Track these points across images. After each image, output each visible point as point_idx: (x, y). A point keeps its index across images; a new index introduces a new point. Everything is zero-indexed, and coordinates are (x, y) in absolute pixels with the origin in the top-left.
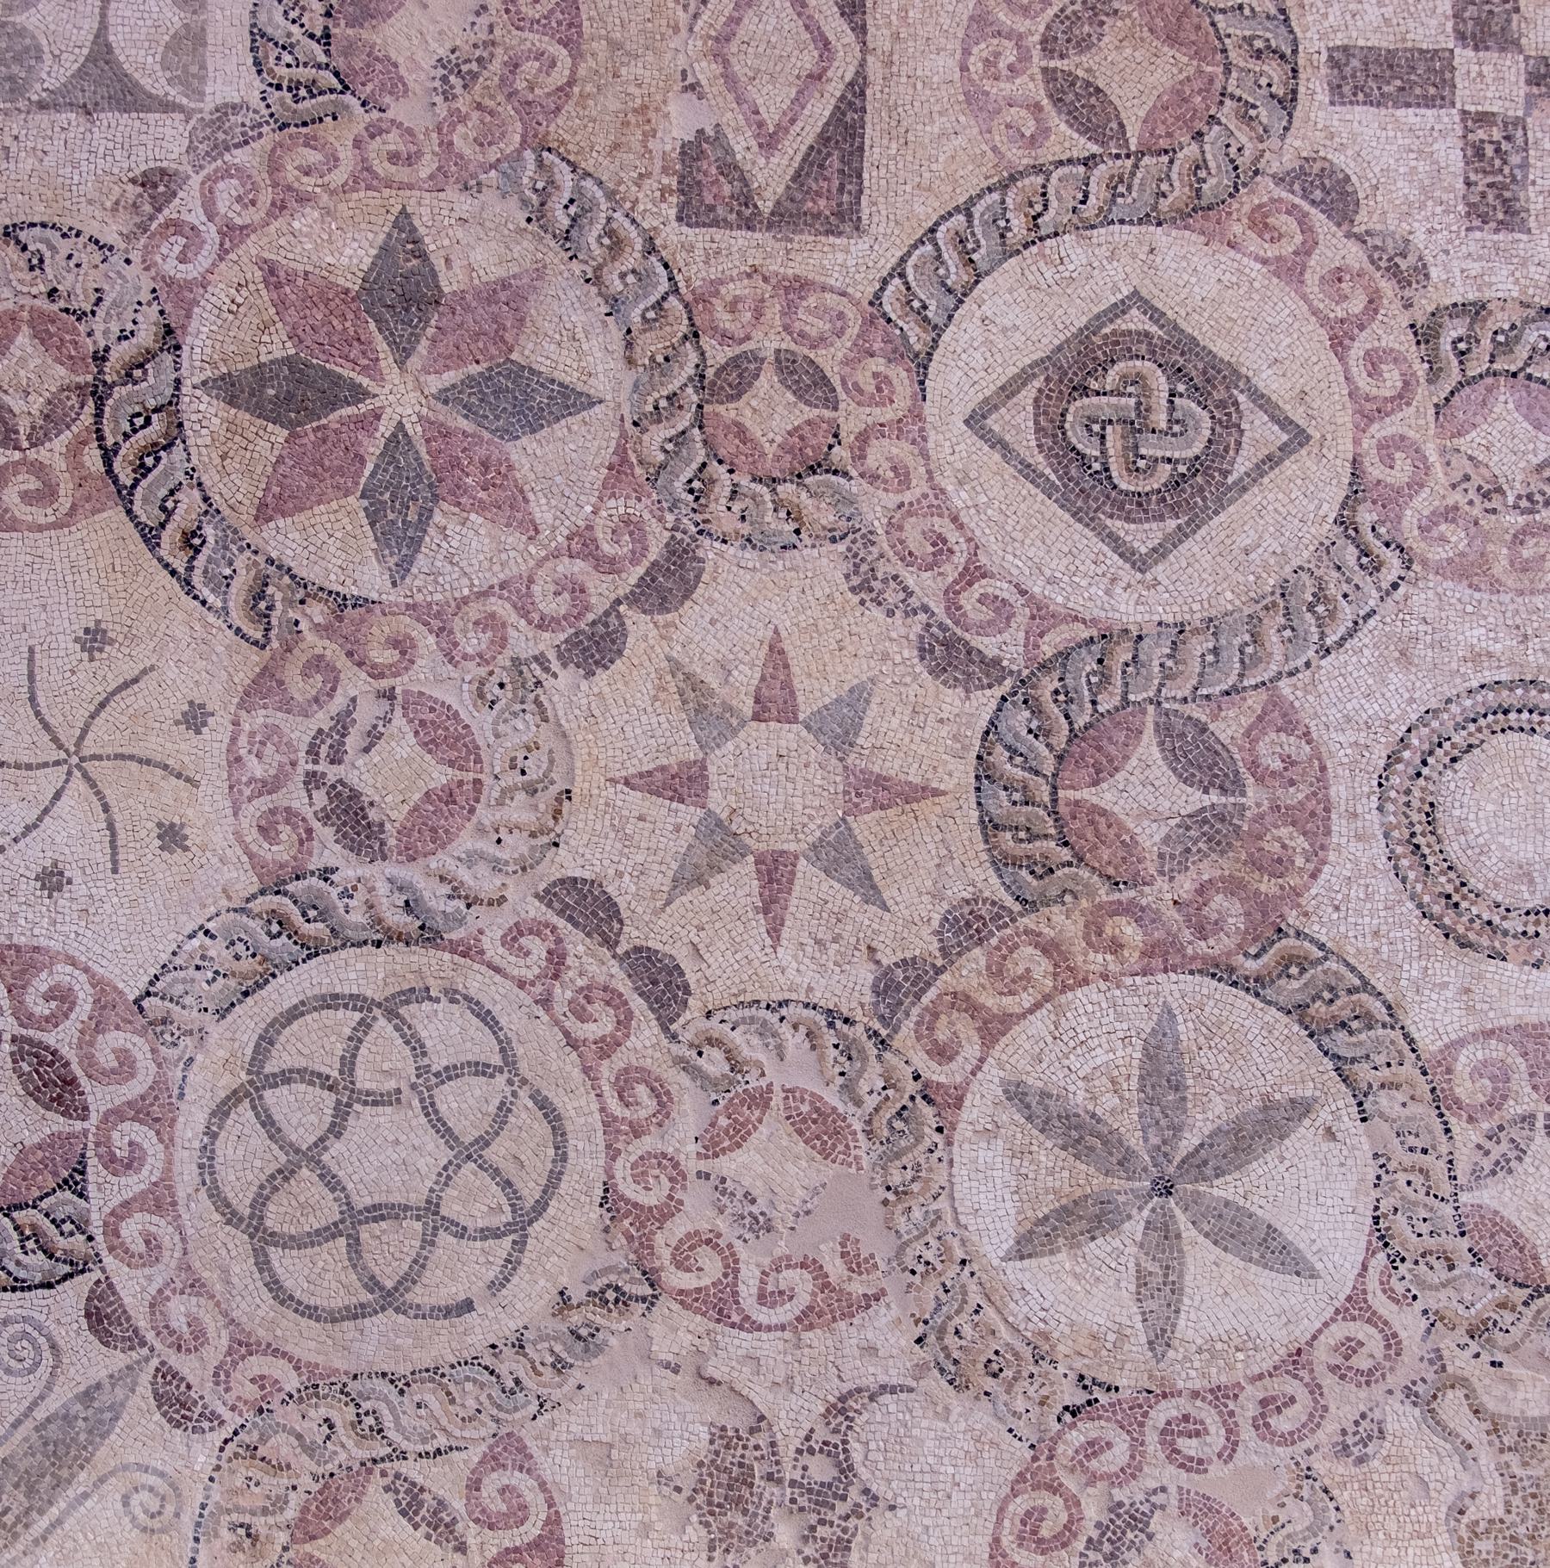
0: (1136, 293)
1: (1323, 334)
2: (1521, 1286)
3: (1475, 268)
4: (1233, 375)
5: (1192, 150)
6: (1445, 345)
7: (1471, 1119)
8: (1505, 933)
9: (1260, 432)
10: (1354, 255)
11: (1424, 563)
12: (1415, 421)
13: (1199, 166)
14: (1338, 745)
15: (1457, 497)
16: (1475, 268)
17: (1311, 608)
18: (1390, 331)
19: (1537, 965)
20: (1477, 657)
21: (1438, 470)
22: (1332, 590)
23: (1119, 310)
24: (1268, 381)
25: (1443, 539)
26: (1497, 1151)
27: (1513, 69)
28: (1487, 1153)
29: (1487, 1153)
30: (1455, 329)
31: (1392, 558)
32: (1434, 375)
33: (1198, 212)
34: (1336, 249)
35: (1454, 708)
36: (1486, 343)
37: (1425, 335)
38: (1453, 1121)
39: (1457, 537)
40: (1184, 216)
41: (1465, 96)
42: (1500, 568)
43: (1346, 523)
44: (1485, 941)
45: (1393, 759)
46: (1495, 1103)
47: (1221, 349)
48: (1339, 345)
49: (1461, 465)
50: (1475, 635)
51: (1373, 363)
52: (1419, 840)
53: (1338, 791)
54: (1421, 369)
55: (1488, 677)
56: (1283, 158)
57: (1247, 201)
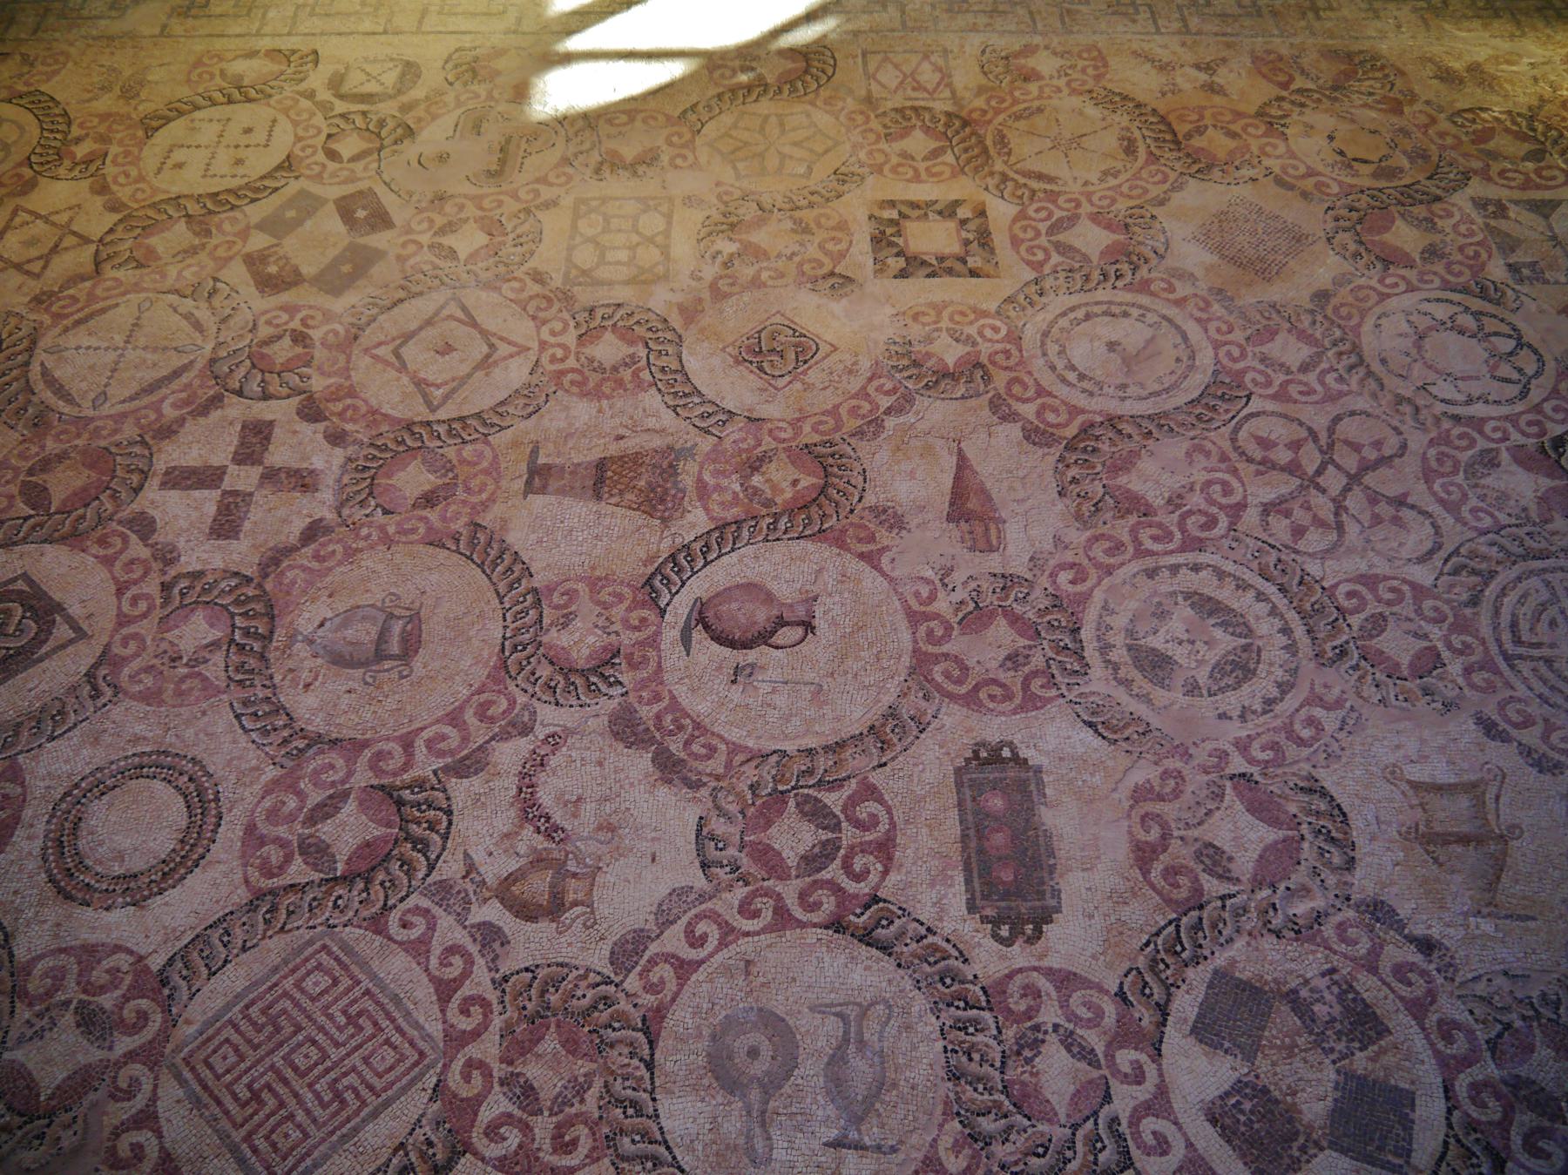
0: (25, 574)
1: (114, 588)
2: (22, 1115)
3: (205, 556)
4: (59, 608)
5: (81, 511)
6: (176, 591)
7: (30, 1005)
8: (96, 890)
9: (62, 631)
10: (145, 553)
11: (126, 693)
12: (146, 628)
13: (83, 517)
14: (37, 786)
15: (156, 662)
16: (205, 556)
17: (53, 717)
18: (152, 587)
19: (107, 909)
20: (136, 740)
21: (150, 650)
22: (68, 708)
23: (15, 580)
24: (75, 610)
25: (141, 681)
26: (39, 1024)
27: (255, 472)
28: (32, 1026)
29: (32, 1026)
30: (184, 583)
31: (109, 692)
32: (167, 600)
33: (74, 539)
34: (138, 549)
35: (114, 767)
36: (198, 589)
37: (166, 587)
38: (18, 1005)
39: (148, 680)
40: (63, 539)
41: (227, 484)
42: (168, 695)
43: (90, 676)
44: (80, 895)
45: (66, 794)
46: (49, 994)
47: (57, 597)
48: (120, 592)
49: (164, 646)
50: (139, 729)
51: (134, 601)
52: (65, 838)
53: (28, 813)
54: (158, 601)
55: (139, 749)
56: (124, 514)
57: (100, 532)
